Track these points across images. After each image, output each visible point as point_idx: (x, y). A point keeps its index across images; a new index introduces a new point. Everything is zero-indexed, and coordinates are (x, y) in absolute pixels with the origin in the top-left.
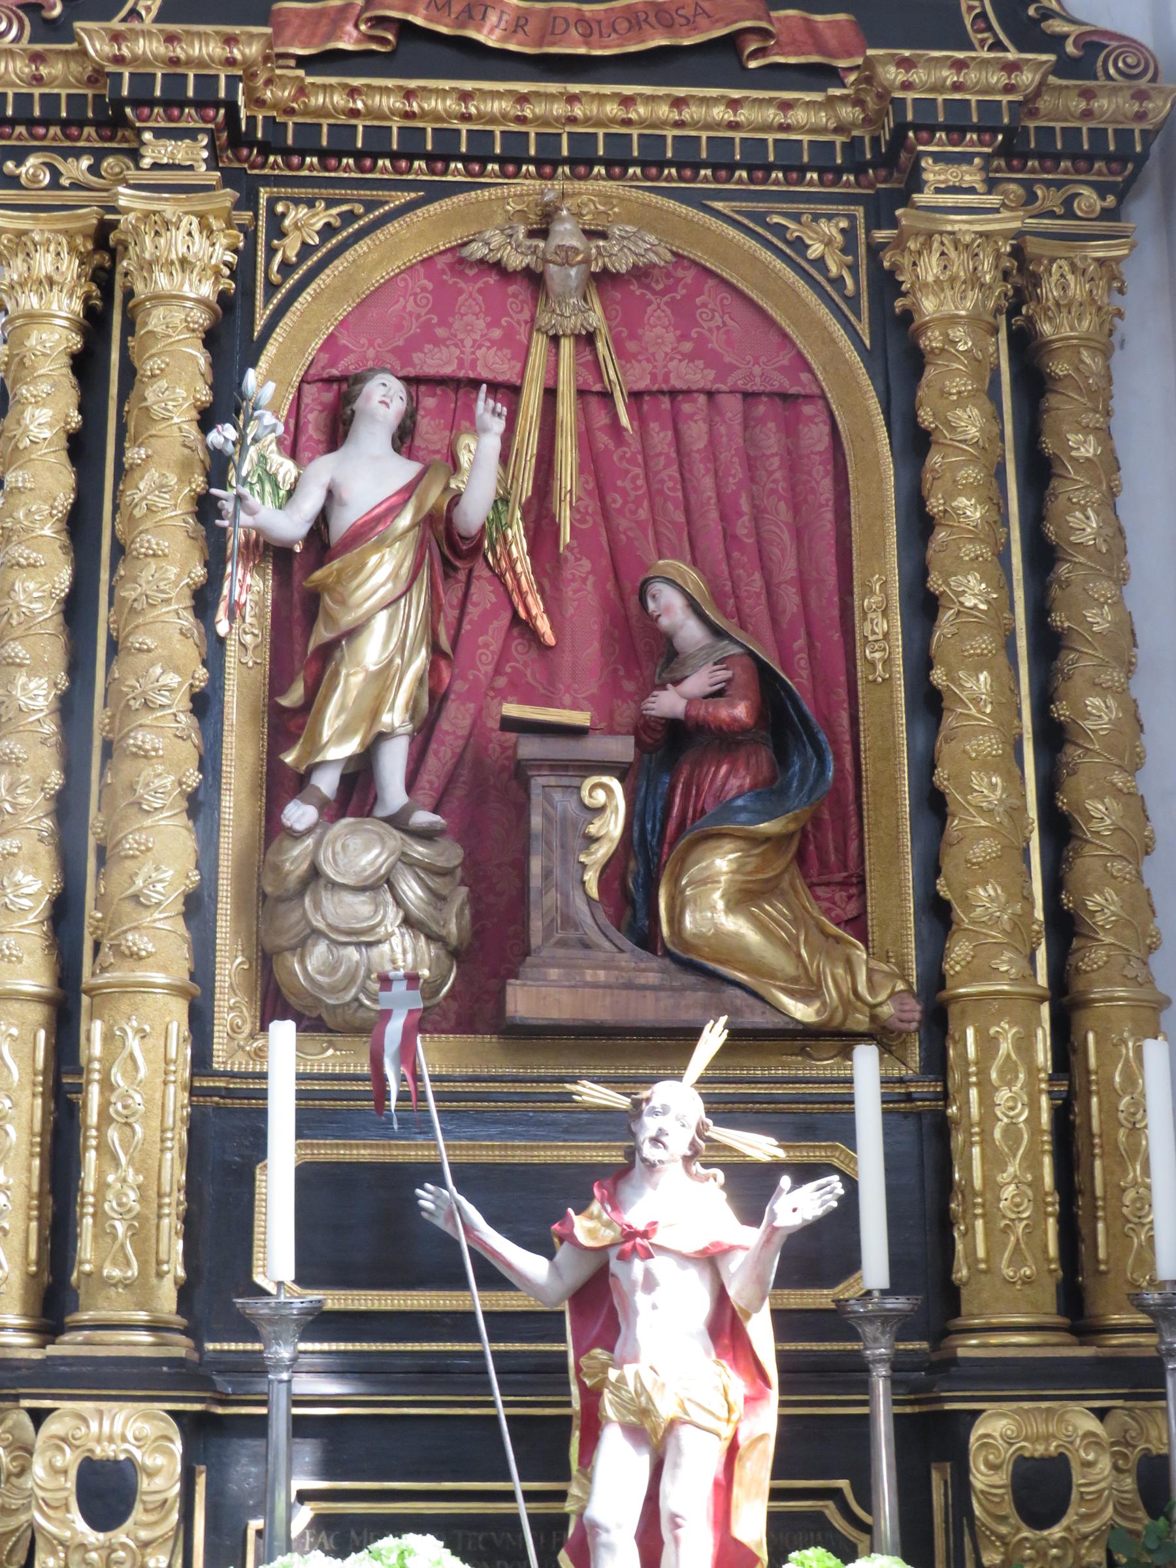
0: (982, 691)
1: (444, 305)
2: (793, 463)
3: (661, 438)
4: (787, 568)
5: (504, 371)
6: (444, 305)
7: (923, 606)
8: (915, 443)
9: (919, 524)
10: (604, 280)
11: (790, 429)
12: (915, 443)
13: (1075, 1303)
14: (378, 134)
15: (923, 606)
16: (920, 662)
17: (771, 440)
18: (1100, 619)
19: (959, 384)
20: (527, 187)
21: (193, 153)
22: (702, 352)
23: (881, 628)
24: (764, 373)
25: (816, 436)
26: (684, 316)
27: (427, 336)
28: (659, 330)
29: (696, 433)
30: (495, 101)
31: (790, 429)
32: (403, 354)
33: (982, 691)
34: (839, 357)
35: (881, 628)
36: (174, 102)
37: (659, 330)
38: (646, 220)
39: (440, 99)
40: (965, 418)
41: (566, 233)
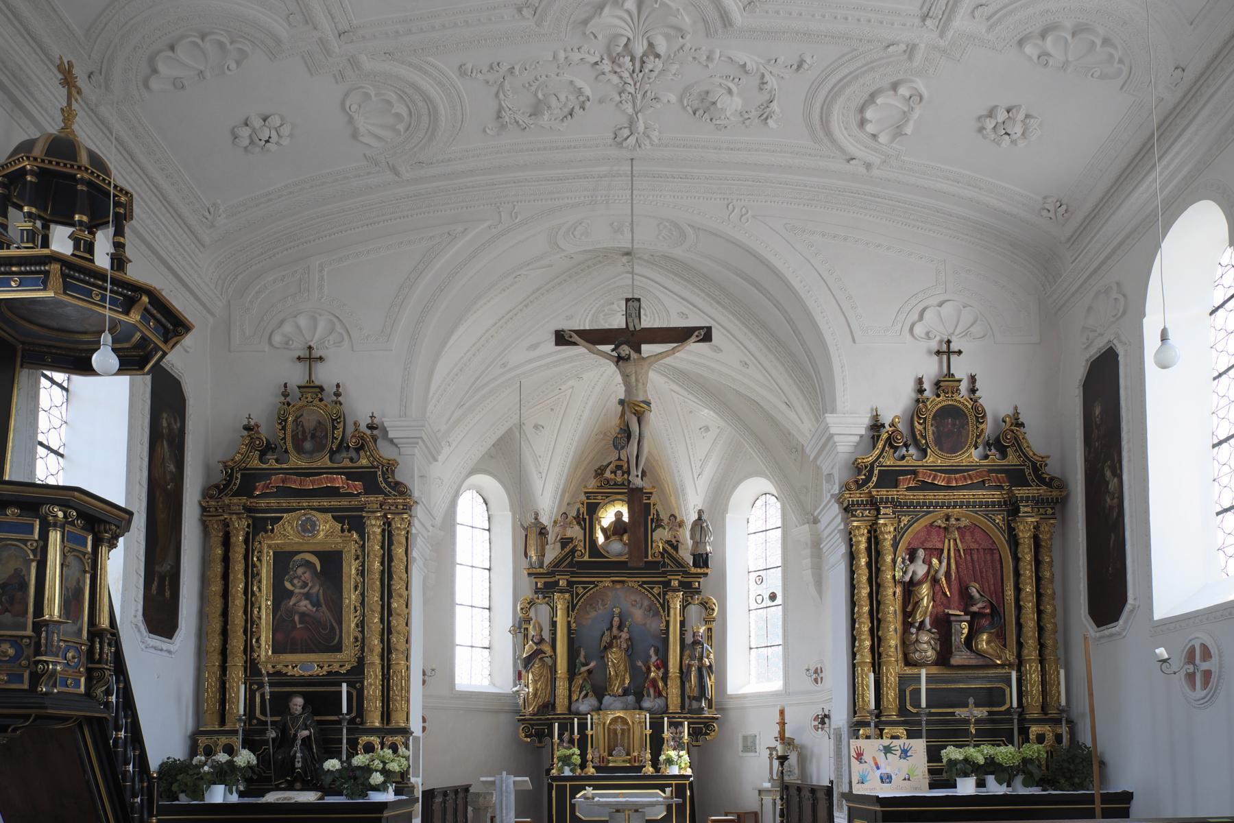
0: (1029, 606)
1: (929, 533)
2: (993, 561)
3: (968, 558)
4: (992, 582)
5: (939, 545)
6: (929, 533)
7: (1018, 590)
8: (1017, 560)
9: (1017, 574)
10: (959, 528)
11: (992, 554)
12: (1017, 560)
13: (1044, 708)
14: (918, 503)
15: (1018, 590)
16: (1017, 600)
17: (989, 557)
18: (1049, 592)
19: (1027, 550)
20: (945, 510)
21: (889, 511)
22: (976, 541)
23: (1010, 593)
24: (986, 544)
25: (997, 557)
26: (972, 534)
27: (926, 540)
28: (968, 537)
29: (975, 557)
30: (940, 496)
31: (992, 554)
32: (922, 543)
33: (1029, 606)
34: (1002, 541)
35: (1010, 593)
36: (886, 503)
37: (968, 537)
38: (966, 517)
39: (931, 496)
40: (1027, 557)
41: (953, 521)
